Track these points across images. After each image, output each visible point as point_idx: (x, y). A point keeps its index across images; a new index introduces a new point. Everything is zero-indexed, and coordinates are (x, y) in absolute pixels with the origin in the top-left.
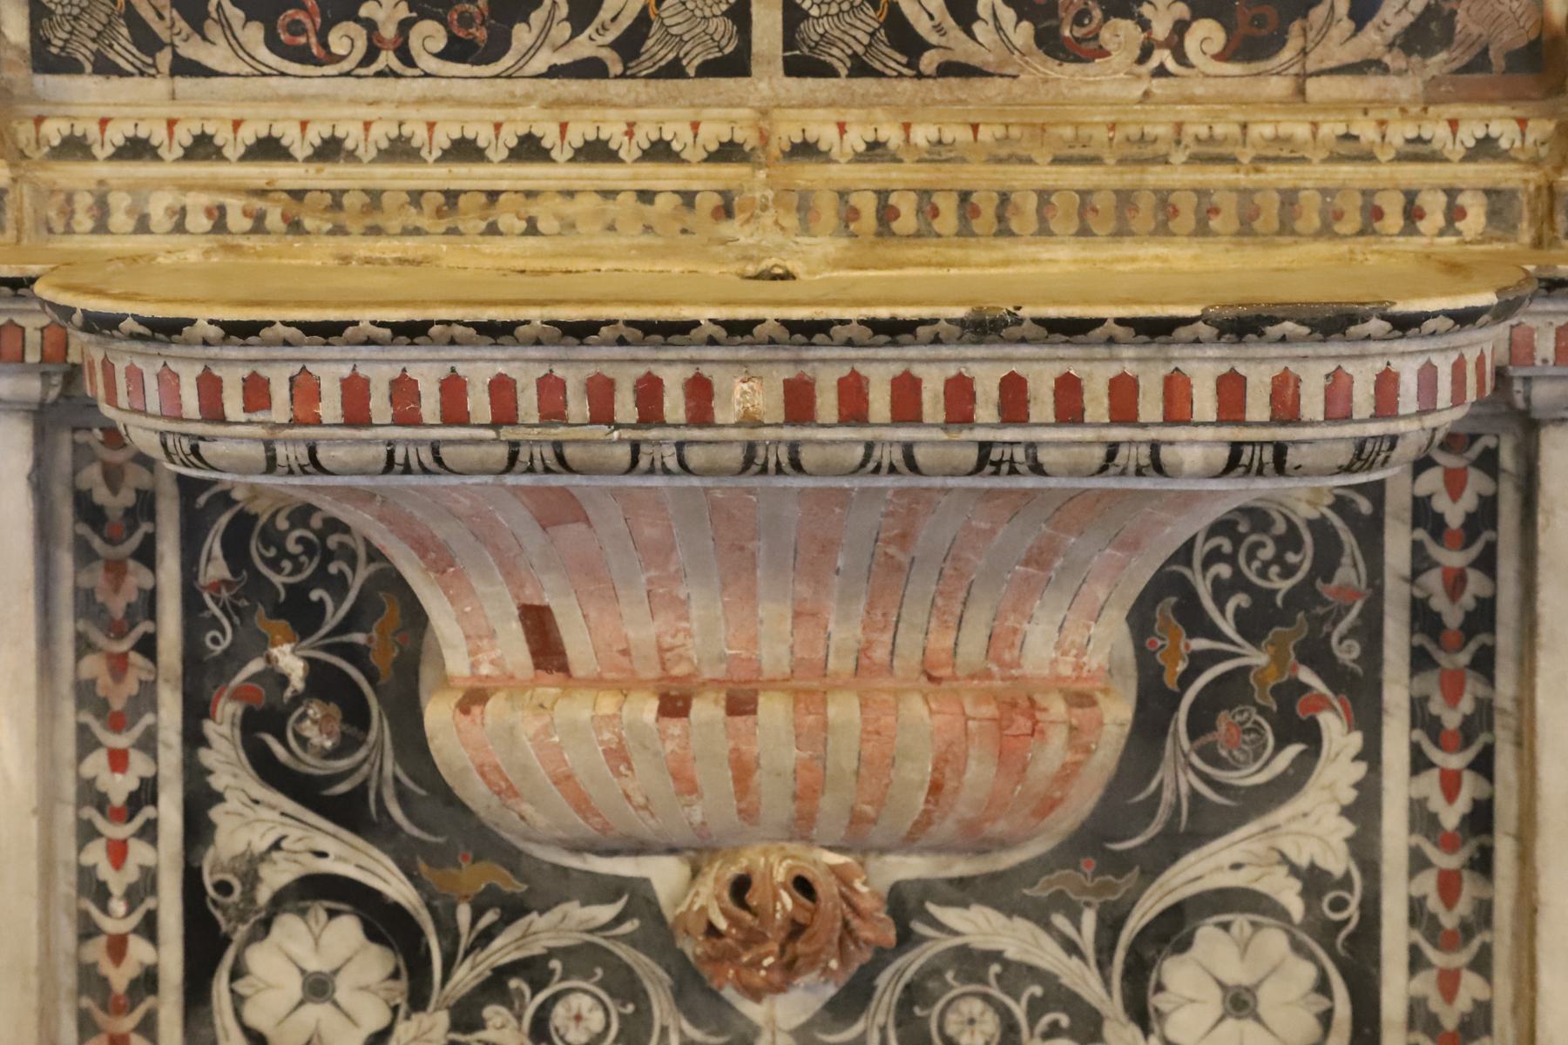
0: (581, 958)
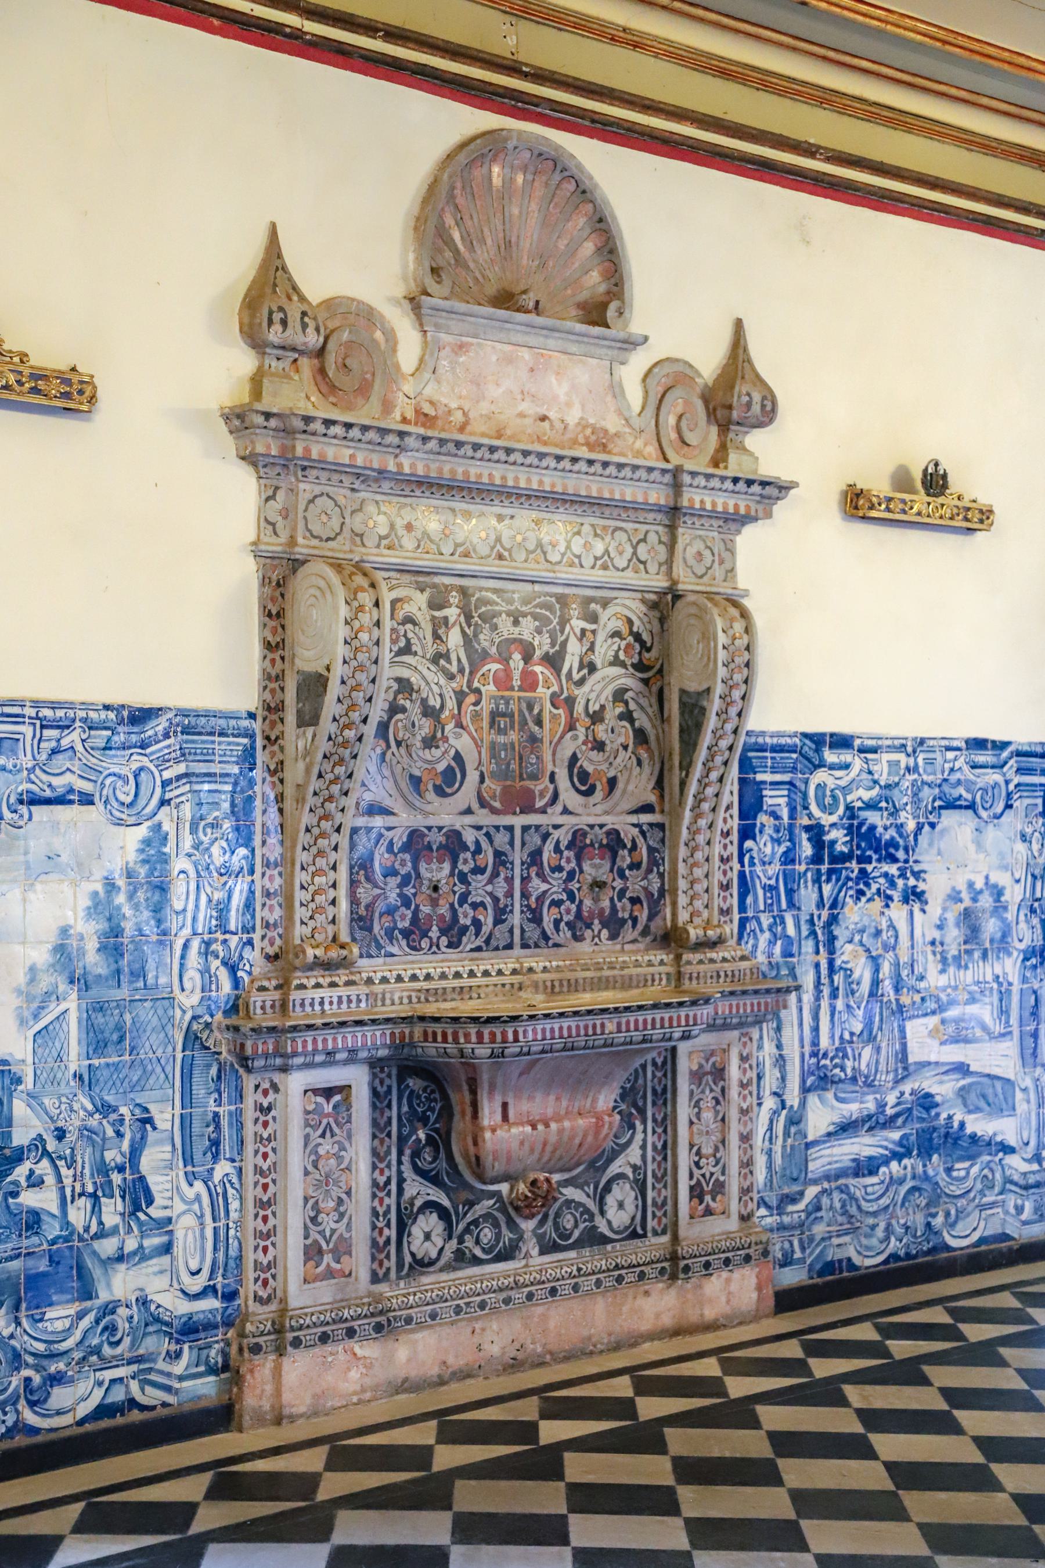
0: (487, 1216)
